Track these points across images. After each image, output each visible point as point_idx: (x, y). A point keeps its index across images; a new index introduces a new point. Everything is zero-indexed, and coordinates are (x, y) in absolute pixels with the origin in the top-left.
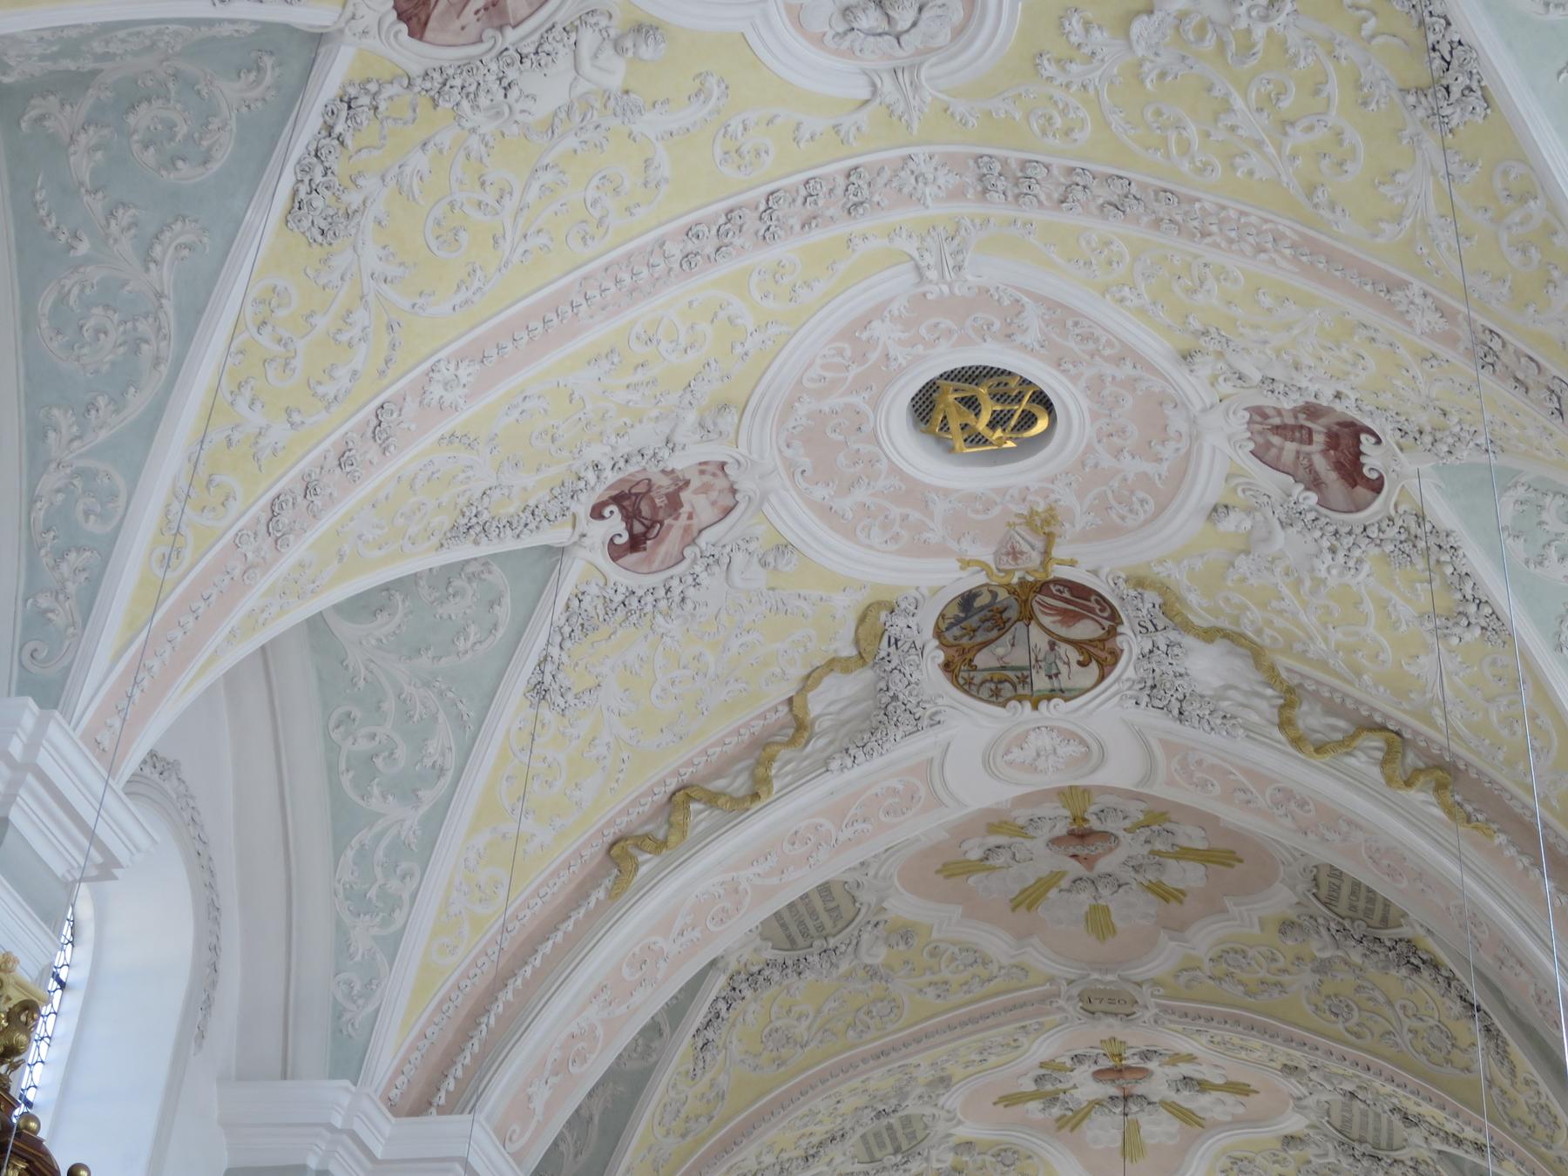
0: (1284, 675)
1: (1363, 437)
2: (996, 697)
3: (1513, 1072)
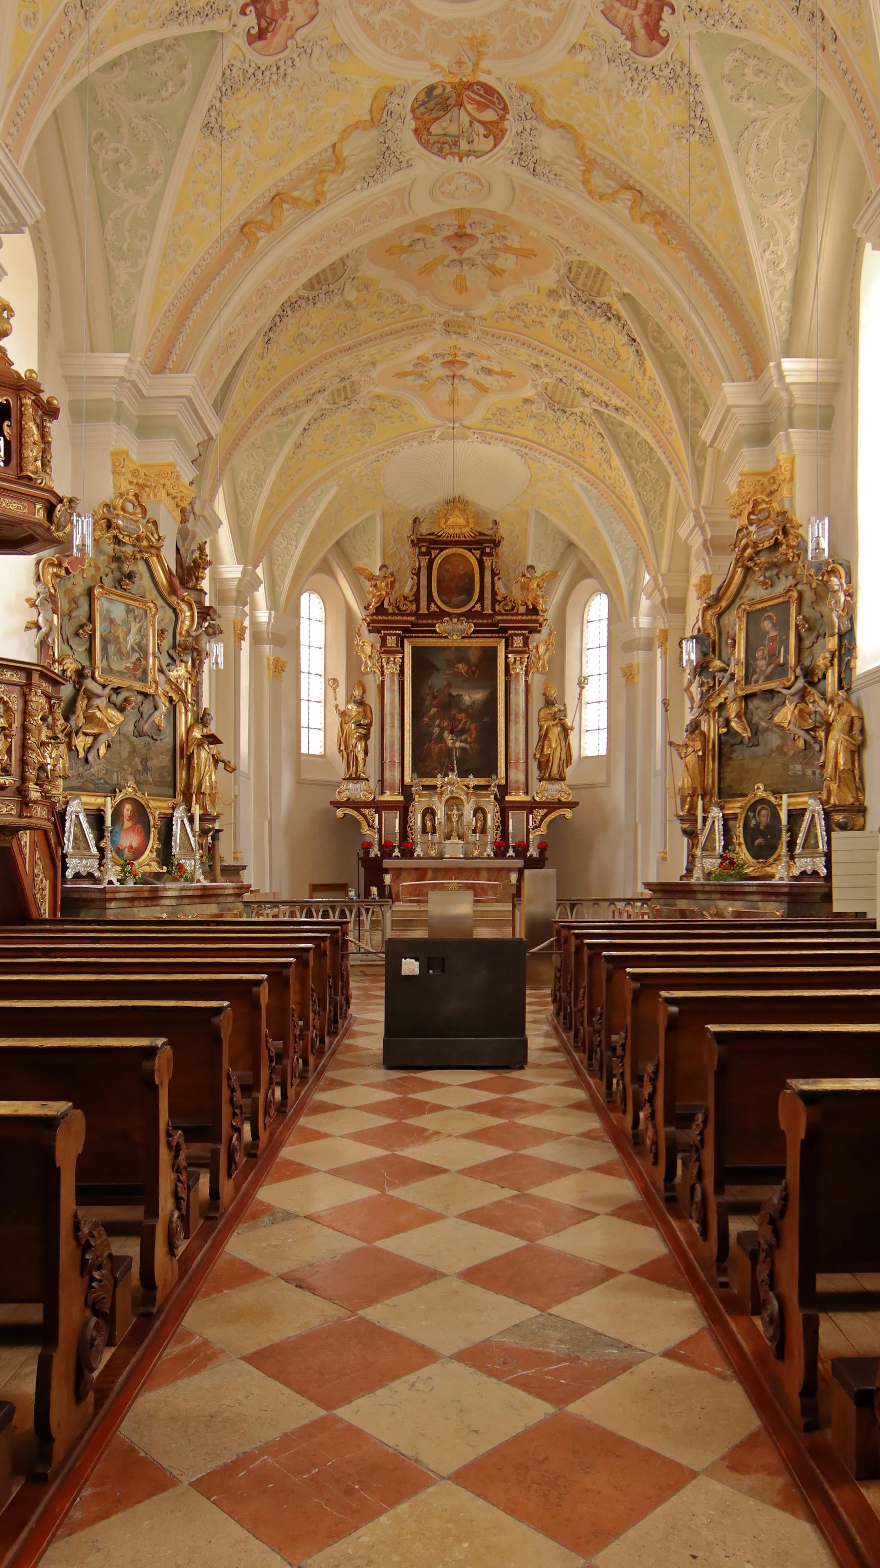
0: (588, 152)
1: (666, 8)
2: (440, 153)
3: (644, 374)
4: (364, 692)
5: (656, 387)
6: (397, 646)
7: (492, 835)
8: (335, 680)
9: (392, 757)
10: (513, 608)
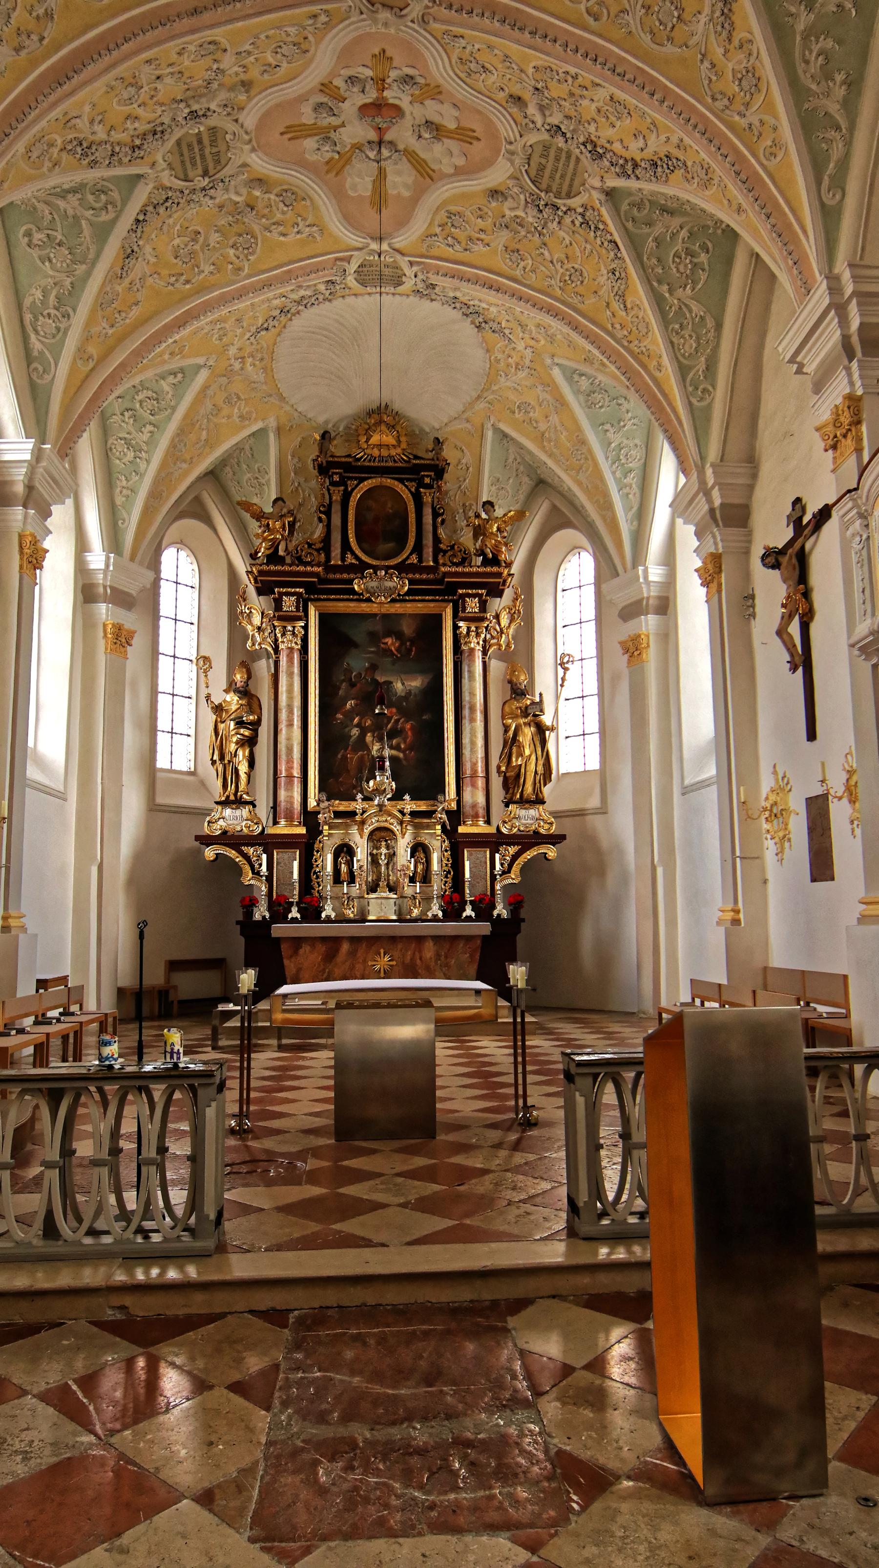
4: (249, 677)
6: (298, 610)
7: (437, 885)
8: (206, 659)
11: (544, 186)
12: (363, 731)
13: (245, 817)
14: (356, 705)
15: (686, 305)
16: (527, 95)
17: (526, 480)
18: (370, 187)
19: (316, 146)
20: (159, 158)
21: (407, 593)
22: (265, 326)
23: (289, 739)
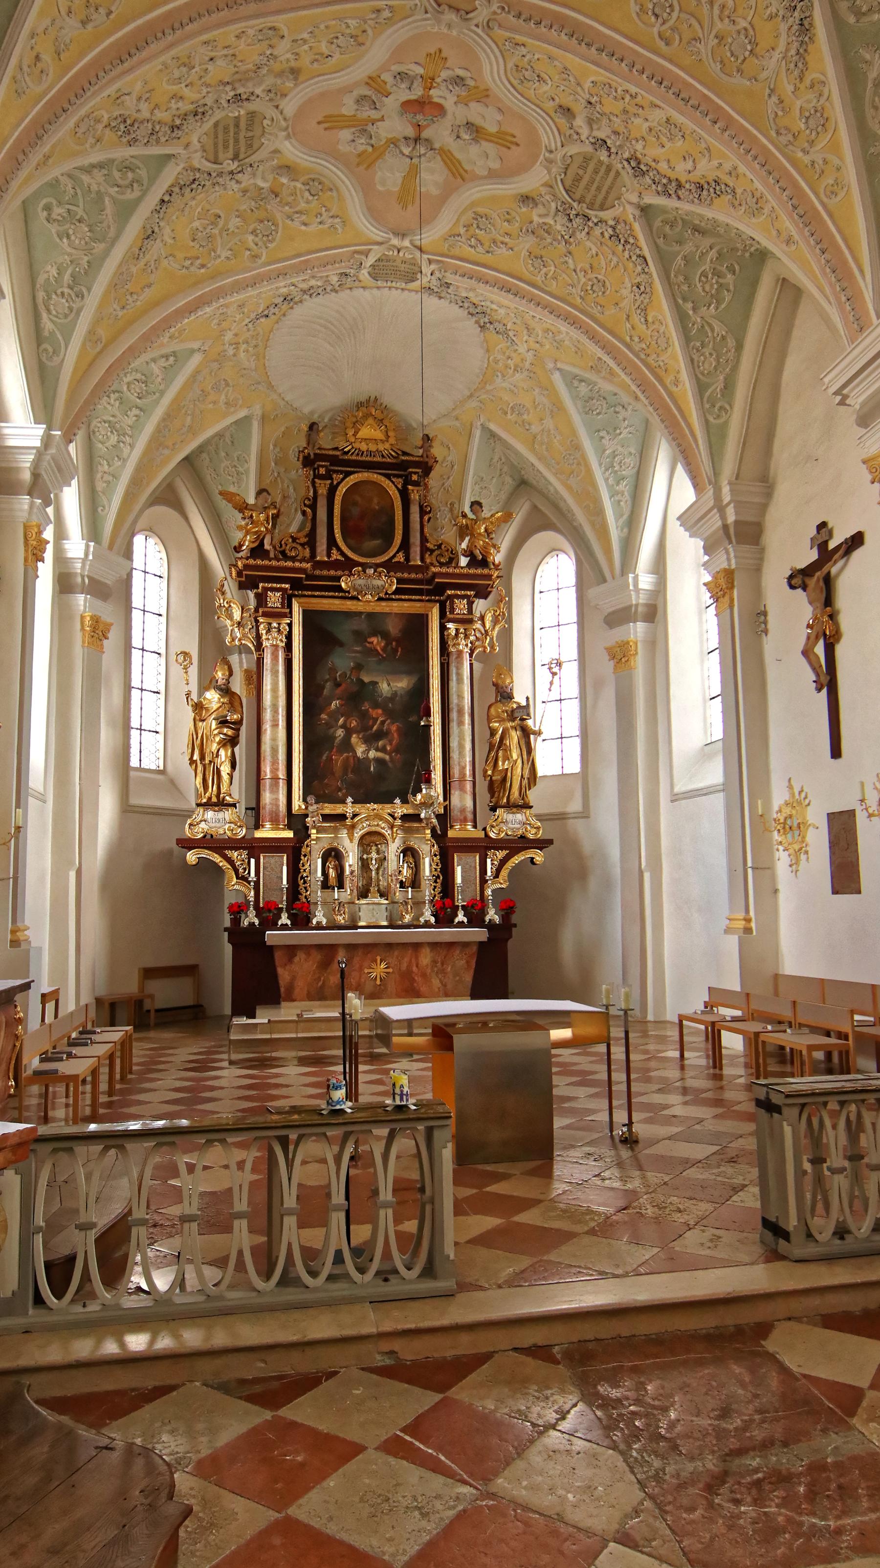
5: (822, 101)
6: (283, 607)
7: (428, 891)
8: (185, 654)
9: (274, 770)
10: (451, 560)
11: (577, 196)
12: (349, 732)
13: (227, 819)
14: (341, 705)
15: (710, 325)
16: (579, 108)
17: (508, 480)
18: (400, 181)
19: (350, 137)
20: (194, 139)
21: (395, 593)
22: (266, 313)
23: (274, 739)
